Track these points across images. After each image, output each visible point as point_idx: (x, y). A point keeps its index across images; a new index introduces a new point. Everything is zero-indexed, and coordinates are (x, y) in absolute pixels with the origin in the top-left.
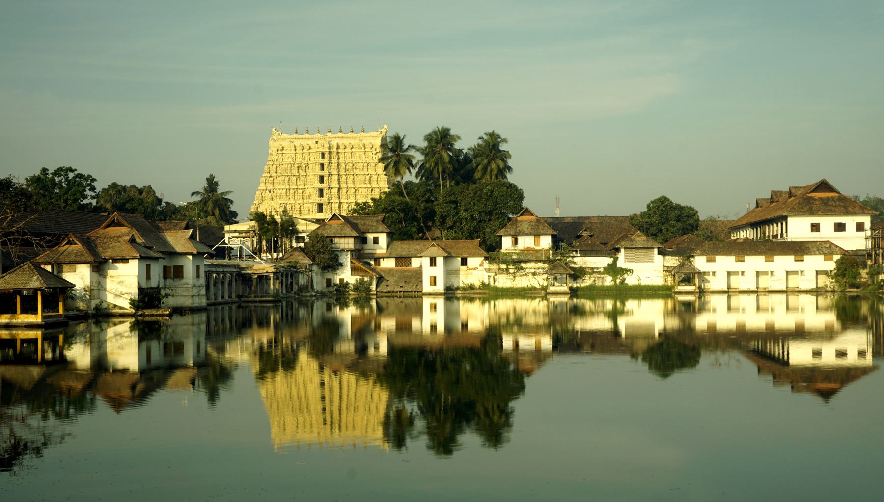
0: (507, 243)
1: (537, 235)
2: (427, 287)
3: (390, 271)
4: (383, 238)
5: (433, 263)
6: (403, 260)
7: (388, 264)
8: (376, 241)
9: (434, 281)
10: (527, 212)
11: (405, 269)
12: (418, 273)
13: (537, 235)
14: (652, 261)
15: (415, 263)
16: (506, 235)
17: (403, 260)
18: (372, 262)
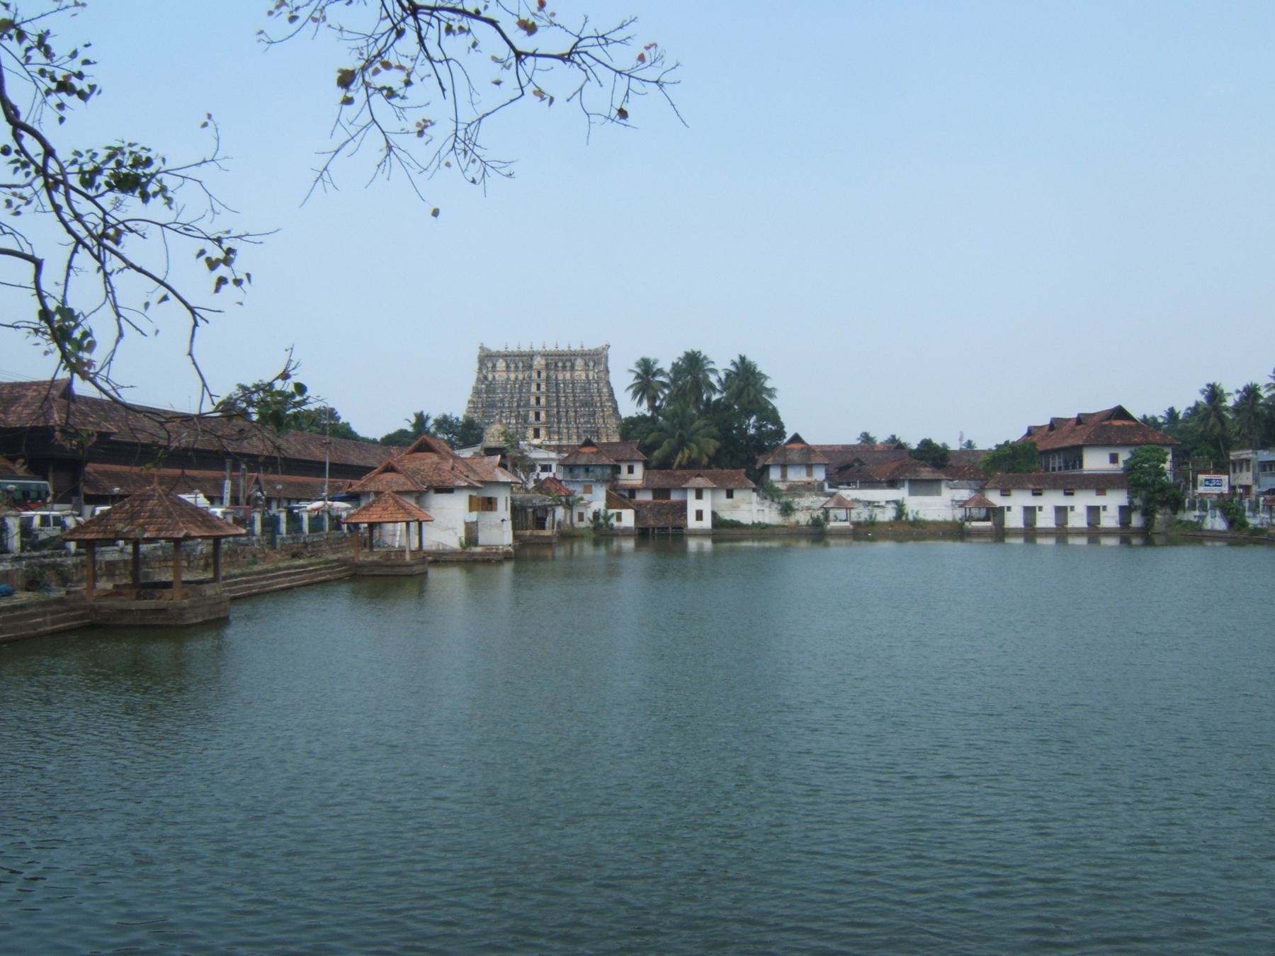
0: (775, 475)
1: (809, 467)
2: (692, 523)
3: (647, 503)
4: (639, 470)
5: (699, 495)
6: (662, 493)
7: (645, 497)
8: (631, 470)
9: (699, 515)
10: (796, 439)
11: (664, 502)
12: (683, 507)
13: (809, 467)
14: (939, 494)
15: (675, 497)
16: (775, 465)
17: (662, 493)
18: (627, 494)
